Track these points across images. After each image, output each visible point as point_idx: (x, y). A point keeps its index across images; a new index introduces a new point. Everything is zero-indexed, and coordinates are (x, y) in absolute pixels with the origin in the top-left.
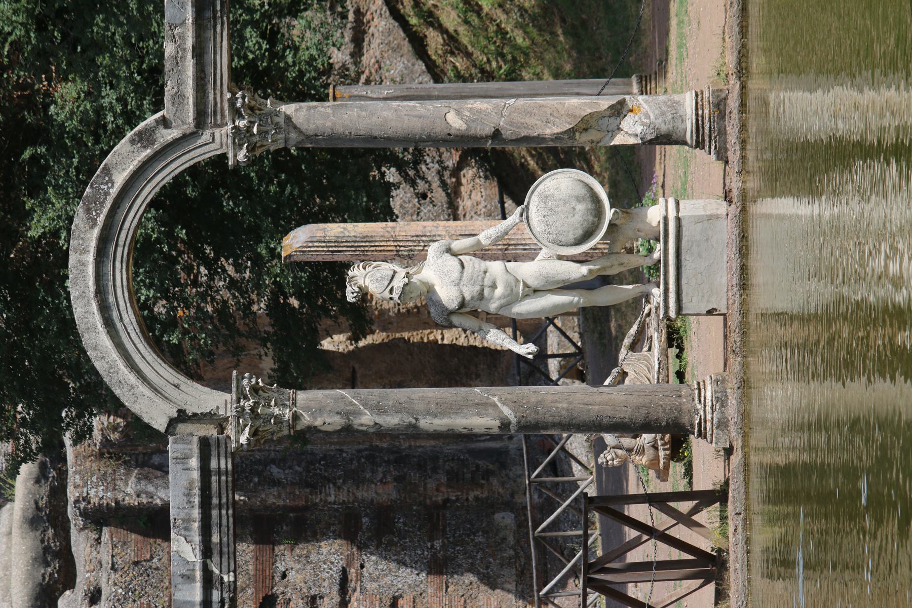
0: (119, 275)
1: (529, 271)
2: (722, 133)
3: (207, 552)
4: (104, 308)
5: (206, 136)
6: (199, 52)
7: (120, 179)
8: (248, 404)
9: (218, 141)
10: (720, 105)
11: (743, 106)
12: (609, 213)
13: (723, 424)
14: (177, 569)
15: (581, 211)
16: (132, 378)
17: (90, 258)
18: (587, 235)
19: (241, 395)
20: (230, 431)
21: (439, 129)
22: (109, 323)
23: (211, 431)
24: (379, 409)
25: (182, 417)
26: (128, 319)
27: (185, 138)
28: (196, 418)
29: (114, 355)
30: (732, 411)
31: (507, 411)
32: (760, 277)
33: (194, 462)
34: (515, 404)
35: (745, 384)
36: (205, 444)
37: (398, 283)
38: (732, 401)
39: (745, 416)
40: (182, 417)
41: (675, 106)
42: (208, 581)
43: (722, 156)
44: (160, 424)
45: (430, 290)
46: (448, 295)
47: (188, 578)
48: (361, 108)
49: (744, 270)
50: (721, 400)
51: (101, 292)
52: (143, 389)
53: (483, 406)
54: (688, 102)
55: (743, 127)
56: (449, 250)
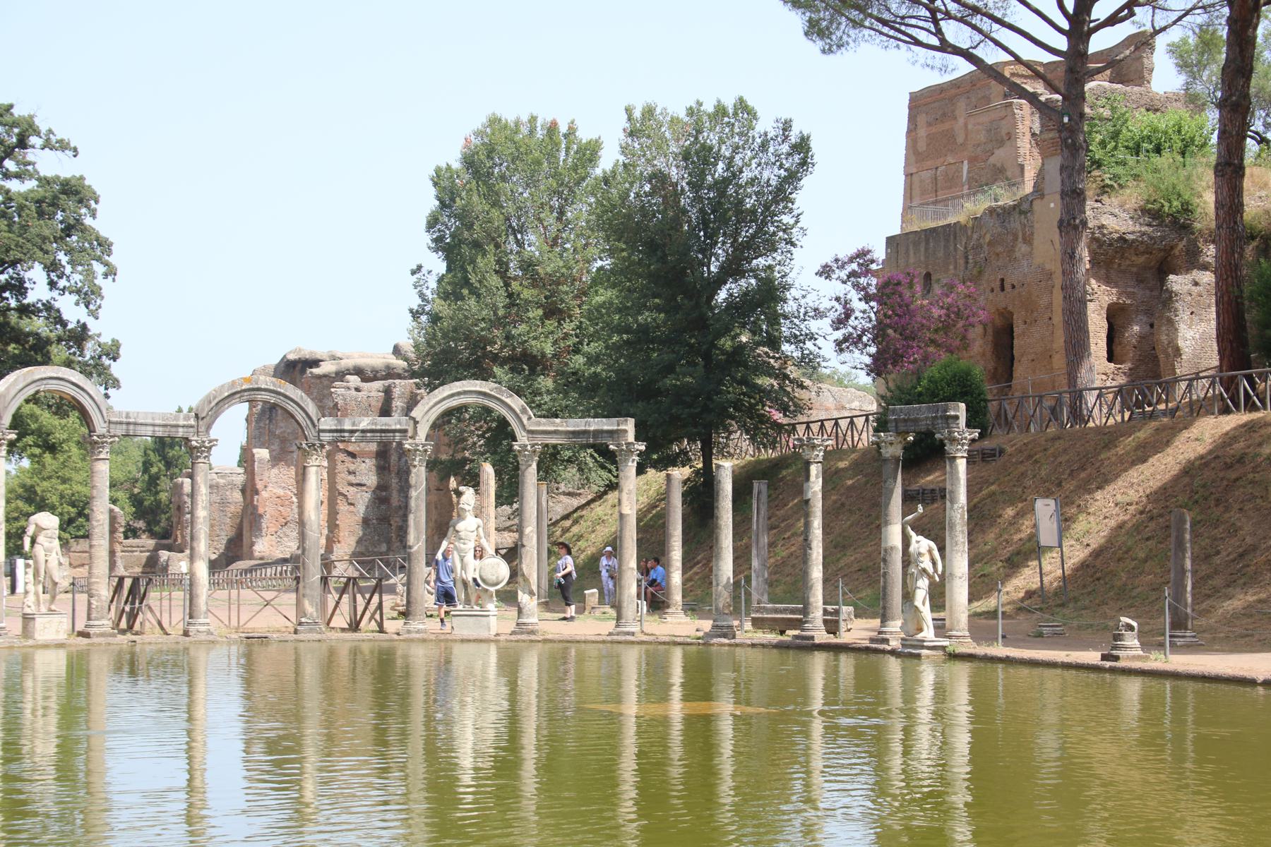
2: (522, 633)
3: (363, 431)
4: (459, 394)
6: (555, 432)
7: (508, 401)
8: (420, 448)
9: (522, 439)
10: (532, 632)
11: (532, 641)
12: (492, 589)
13: (409, 632)
14: (357, 419)
15: (492, 578)
16: (431, 404)
17: (478, 389)
18: (483, 580)
19: (424, 445)
20: (410, 441)
21: (525, 524)
22: (452, 395)
23: (410, 434)
24: (417, 498)
25: (416, 423)
27: (523, 426)
28: (415, 428)
29: (441, 397)
31: (415, 548)
32: (465, 646)
33: (398, 427)
34: (417, 552)
35: (424, 641)
36: (405, 431)
38: (418, 636)
39: (412, 640)
40: (416, 423)
41: (533, 615)
42: (352, 432)
43: (513, 633)
44: (413, 414)
47: (354, 424)
49: (469, 641)
50: (418, 632)
51: (465, 392)
52: (427, 408)
53: (418, 539)
54: (534, 620)
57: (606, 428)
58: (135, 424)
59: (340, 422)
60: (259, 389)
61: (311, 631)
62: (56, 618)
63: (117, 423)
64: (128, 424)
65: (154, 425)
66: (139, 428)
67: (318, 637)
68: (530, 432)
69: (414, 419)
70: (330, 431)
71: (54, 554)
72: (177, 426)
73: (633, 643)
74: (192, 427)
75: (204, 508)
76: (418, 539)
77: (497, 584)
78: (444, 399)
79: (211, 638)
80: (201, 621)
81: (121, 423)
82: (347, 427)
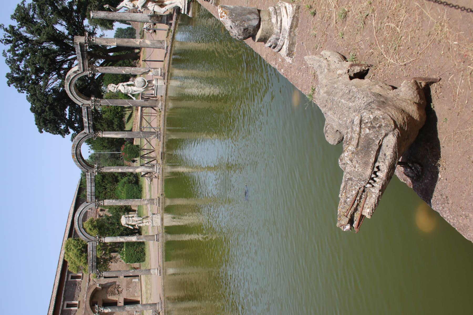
0: (73, 88)
1: (134, 88)
2: (164, 77)
3: (88, 120)
4: (71, 92)
5: (85, 72)
6: (83, 63)
11: (168, 76)
12: (147, 83)
15: (143, 84)
19: (92, 102)
21: (121, 73)
26: (74, 93)
27: (81, 73)
30: (163, 107)
34: (132, 104)
35: (165, 106)
36: (87, 108)
37: (115, 90)
41: (158, 72)
43: (164, 79)
45: (120, 90)
46: (123, 91)
48: (109, 69)
55: (168, 78)
56: (123, 86)
57: (79, 48)
58: (91, 193)
59: (86, 127)
60: (76, 153)
61: (160, 138)
62: (154, 219)
63: (91, 199)
64: (91, 195)
65: (91, 187)
66: (92, 191)
67: (162, 137)
68: (84, 70)
69: (82, 105)
70: (89, 130)
71: (134, 218)
72: (91, 179)
73: (172, 46)
74: (91, 174)
75: (118, 169)
76: (128, 104)
77: (145, 82)
78: (73, 96)
79: (161, 169)
80: (155, 171)
81: (91, 198)
82: (87, 125)
